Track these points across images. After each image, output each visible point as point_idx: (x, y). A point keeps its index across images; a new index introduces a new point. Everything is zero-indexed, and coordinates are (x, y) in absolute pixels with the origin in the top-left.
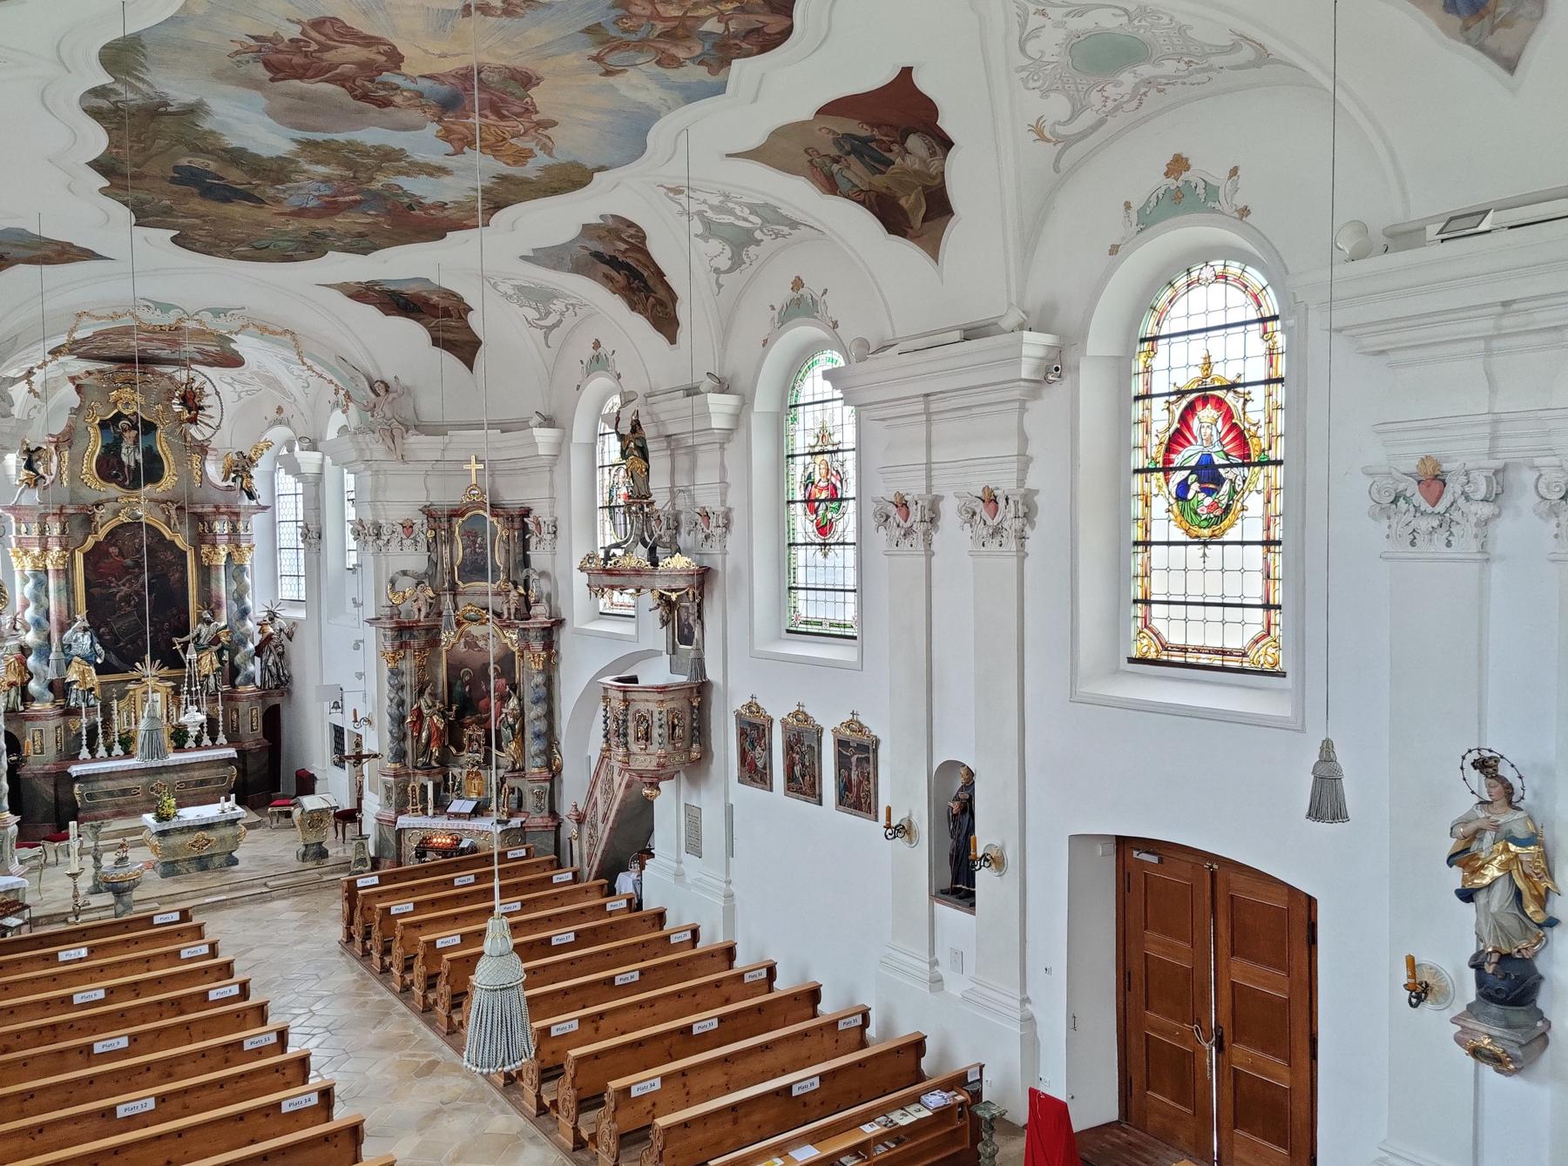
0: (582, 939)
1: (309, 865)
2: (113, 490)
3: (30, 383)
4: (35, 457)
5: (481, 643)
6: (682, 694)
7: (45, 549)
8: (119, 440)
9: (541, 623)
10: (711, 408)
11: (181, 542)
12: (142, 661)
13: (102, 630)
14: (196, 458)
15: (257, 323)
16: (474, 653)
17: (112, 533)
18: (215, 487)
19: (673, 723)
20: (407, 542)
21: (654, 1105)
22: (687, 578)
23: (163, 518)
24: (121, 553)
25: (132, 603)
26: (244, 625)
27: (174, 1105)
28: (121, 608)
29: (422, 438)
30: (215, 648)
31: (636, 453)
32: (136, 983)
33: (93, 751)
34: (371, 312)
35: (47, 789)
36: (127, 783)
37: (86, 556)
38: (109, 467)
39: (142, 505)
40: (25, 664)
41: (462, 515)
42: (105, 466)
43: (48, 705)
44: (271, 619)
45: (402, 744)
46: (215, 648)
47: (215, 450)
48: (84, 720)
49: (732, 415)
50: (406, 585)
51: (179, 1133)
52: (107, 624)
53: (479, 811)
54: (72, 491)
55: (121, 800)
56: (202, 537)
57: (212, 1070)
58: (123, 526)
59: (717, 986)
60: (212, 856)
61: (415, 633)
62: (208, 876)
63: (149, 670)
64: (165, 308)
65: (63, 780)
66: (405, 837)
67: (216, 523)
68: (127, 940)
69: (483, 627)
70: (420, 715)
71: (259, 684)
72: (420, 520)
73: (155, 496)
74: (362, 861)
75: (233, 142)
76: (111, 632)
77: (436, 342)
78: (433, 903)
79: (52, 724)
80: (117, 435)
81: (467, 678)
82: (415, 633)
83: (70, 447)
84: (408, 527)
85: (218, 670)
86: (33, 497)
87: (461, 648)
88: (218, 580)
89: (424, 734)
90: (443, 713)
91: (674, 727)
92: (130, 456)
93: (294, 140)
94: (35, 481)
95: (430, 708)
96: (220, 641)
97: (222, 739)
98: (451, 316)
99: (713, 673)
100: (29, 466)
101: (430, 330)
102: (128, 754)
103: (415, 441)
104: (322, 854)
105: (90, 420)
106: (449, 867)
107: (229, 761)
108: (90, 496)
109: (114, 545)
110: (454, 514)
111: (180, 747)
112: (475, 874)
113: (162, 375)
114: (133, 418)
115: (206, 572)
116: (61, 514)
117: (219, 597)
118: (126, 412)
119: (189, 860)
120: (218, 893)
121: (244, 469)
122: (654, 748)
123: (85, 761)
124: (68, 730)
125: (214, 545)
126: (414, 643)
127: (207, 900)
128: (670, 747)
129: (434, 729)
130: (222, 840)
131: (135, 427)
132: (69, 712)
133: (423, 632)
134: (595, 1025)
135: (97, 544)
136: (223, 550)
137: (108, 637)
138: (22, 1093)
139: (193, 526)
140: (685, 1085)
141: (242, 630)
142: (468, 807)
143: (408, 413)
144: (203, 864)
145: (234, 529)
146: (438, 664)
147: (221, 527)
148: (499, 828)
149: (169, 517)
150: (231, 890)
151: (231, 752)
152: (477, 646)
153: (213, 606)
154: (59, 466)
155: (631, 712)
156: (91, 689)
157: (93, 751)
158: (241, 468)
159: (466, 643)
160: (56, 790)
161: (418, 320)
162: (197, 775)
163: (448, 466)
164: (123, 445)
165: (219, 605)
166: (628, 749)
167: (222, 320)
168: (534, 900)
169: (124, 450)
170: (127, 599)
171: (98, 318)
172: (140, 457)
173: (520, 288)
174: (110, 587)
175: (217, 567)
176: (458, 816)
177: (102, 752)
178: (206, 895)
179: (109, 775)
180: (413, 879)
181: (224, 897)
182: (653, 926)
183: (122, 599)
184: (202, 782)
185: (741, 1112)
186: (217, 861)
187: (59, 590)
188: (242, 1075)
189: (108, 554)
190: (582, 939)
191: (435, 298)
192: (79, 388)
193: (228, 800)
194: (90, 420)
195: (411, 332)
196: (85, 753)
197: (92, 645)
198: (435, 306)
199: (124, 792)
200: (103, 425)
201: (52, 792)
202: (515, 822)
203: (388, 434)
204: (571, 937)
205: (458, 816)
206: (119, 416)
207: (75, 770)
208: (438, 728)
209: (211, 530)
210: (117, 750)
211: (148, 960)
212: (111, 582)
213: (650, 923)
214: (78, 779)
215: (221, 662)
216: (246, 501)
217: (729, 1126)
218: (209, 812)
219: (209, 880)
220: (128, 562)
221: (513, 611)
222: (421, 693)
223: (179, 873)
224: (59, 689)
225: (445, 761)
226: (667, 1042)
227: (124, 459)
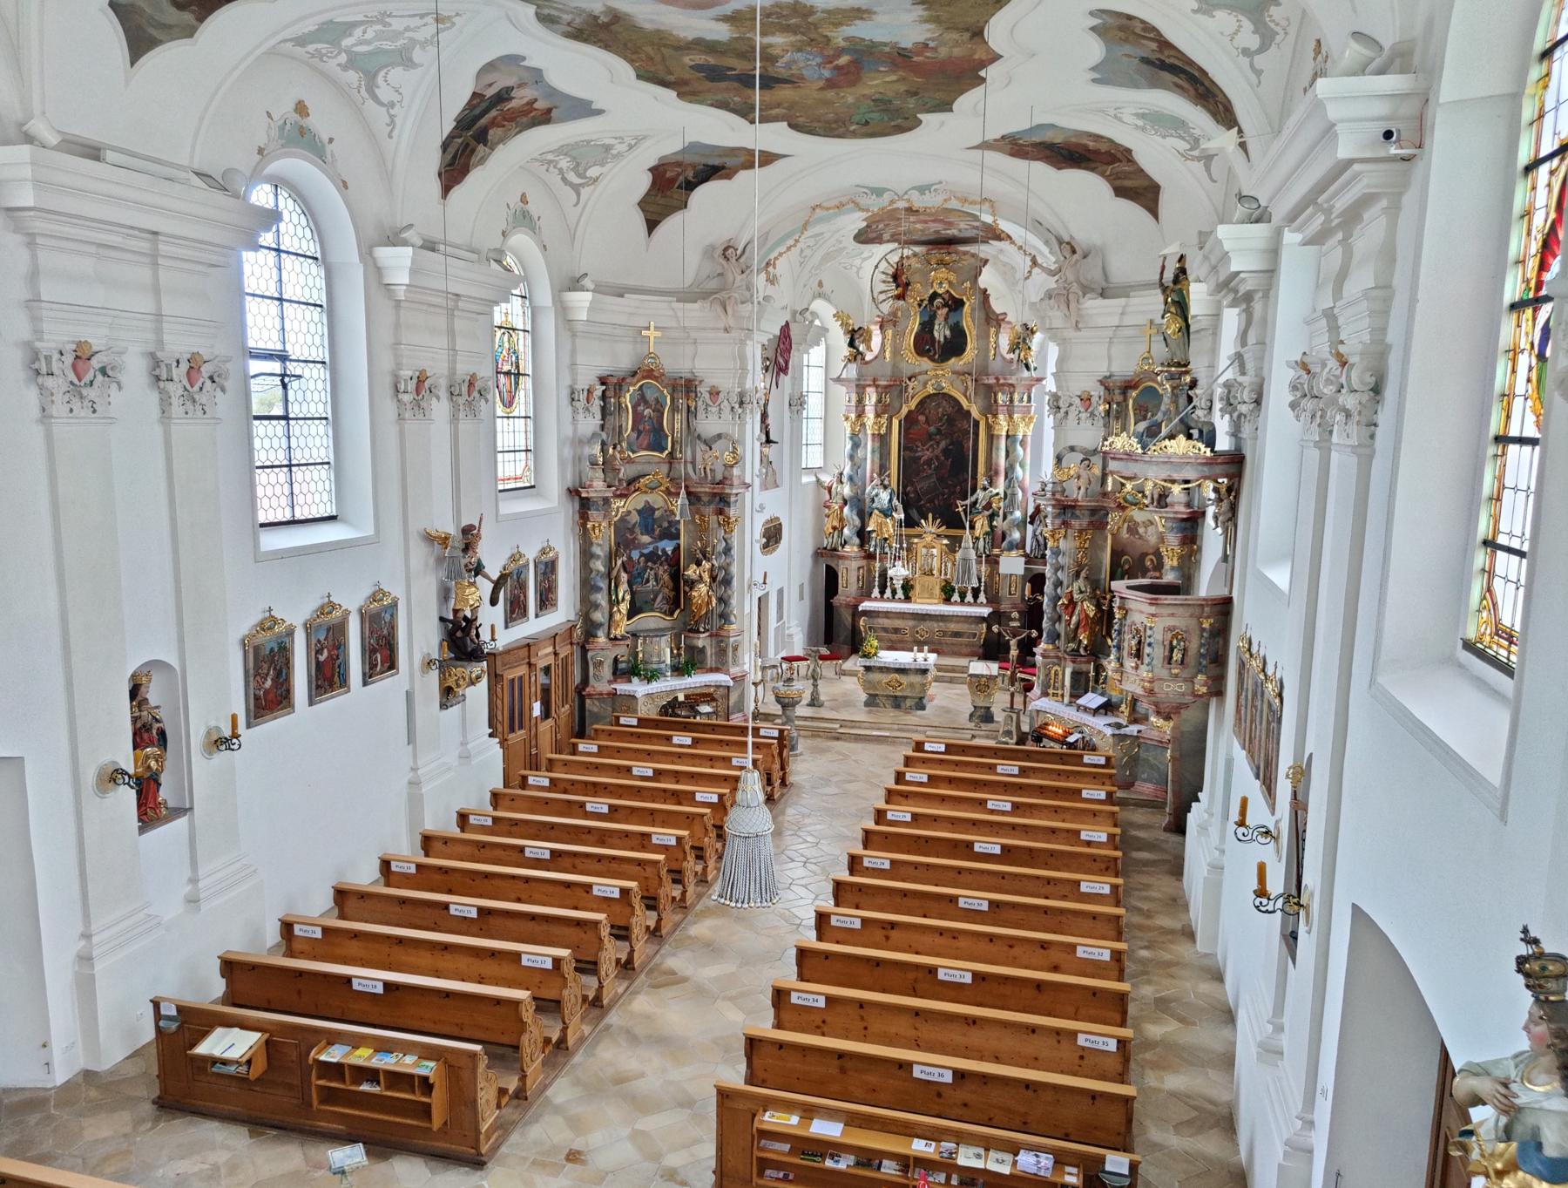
0: (1008, 854)
1: (972, 725)
2: (926, 364)
3: (1041, 266)
4: (856, 336)
5: (1141, 530)
6: (1191, 610)
7: (860, 414)
8: (933, 317)
9: (1176, 513)
10: (1226, 248)
11: (975, 413)
12: (926, 519)
14: (993, 330)
15: (959, 195)
16: (1135, 539)
17: (921, 403)
18: (1004, 358)
19: (1171, 642)
20: (1083, 416)
21: (824, 1022)
22: (1200, 468)
23: (962, 388)
24: (927, 422)
27: (567, 862)
29: (1100, 302)
30: (987, 513)
31: (1173, 309)
32: (677, 772)
33: (882, 592)
34: (1040, 169)
35: (847, 617)
36: (898, 623)
38: (924, 343)
39: (944, 378)
40: (842, 511)
41: (1135, 387)
43: (856, 549)
45: (1057, 625)
46: (987, 513)
47: (1009, 323)
48: (878, 565)
49: (1265, 251)
50: (1073, 462)
51: (527, 880)
53: (1108, 708)
54: (894, 365)
55: (894, 637)
56: (991, 409)
57: (632, 849)
58: (929, 396)
59: (1042, 947)
60: (905, 698)
61: (1078, 512)
62: (897, 713)
63: (929, 527)
64: (879, 192)
65: (856, 614)
66: (1041, 714)
67: (1000, 395)
68: (721, 741)
69: (1143, 513)
70: (1072, 603)
71: (1028, 551)
72: (1097, 392)
73: (957, 368)
74: (1008, 733)
75: (690, 36)
77: (1120, 192)
78: (951, 781)
79: (854, 565)
81: (1127, 567)
82: (1078, 512)
84: (1086, 400)
85: (987, 533)
86: (852, 371)
87: (1124, 534)
88: (998, 449)
89: (1074, 619)
90: (1098, 601)
91: (1172, 650)
92: (941, 332)
93: (718, 20)
94: (856, 356)
95: (1081, 592)
97: (982, 598)
98: (1120, 161)
99: (1235, 595)
100: (851, 344)
101: (1107, 178)
102: (908, 599)
103: (1093, 305)
104: (987, 717)
106: (1020, 755)
107: (983, 619)
108: (907, 370)
109: (922, 413)
110: (1127, 387)
111: (947, 600)
112: (1020, 767)
113: (965, 253)
114: (946, 297)
115: (991, 438)
116: (877, 387)
117: (997, 465)
118: (941, 291)
119: (887, 696)
120: (888, 729)
121: (1024, 340)
122: (1144, 672)
123: (876, 599)
124: (869, 571)
125: (995, 416)
126: (1076, 523)
127: (875, 733)
128: (1164, 673)
129: (1083, 616)
130: (911, 685)
131: (946, 305)
132: (870, 557)
133: (1087, 513)
134: (884, 932)
135: (910, 412)
136: (1002, 419)
138: (511, 819)
139: (988, 397)
140: (862, 1018)
142: (1101, 700)
143: (1096, 274)
144: (897, 702)
145: (1011, 400)
146: (1103, 548)
147: (1001, 398)
148: (1109, 731)
149: (967, 388)
150: (899, 730)
151: (986, 611)
152: (1138, 533)
154: (883, 344)
155: (1128, 622)
156: (886, 539)
157: (882, 592)
158: (1021, 343)
159: (1129, 530)
160: (853, 620)
161: (1092, 170)
162: (953, 627)
163: (1130, 332)
164: (937, 322)
165: (997, 473)
166: (1122, 665)
167: (927, 197)
168: (1031, 806)
169: (936, 327)
170: (929, 462)
171: (828, 209)
172: (948, 333)
173: (1142, 116)
175: (999, 437)
176: (1086, 709)
177: (888, 593)
178: (879, 729)
179: (887, 614)
180: (982, 757)
181: (887, 734)
182: (1107, 869)
184: (956, 634)
185: (849, 1064)
186: (909, 703)
187: (873, 451)
188: (614, 858)
189: (917, 421)
190: (1008, 854)
191: (1091, 145)
193: (921, 650)
195: (1087, 186)
196: (876, 593)
197: (890, 500)
198: (1097, 152)
199: (896, 631)
201: (850, 619)
202: (1133, 729)
203: (1062, 299)
204: (997, 850)
205: (1086, 709)
206: (934, 296)
207: (866, 605)
208: (1087, 616)
209: (996, 401)
210: (900, 594)
211: (711, 758)
213: (1103, 866)
214: (866, 613)
215: (991, 526)
216: (1026, 374)
217: (834, 1071)
218: (903, 658)
219: (888, 716)
220: (932, 429)
221: (1156, 497)
222: (1077, 575)
223: (877, 705)
224: (863, 535)
225: (1097, 651)
226: (911, 975)
227: (936, 334)
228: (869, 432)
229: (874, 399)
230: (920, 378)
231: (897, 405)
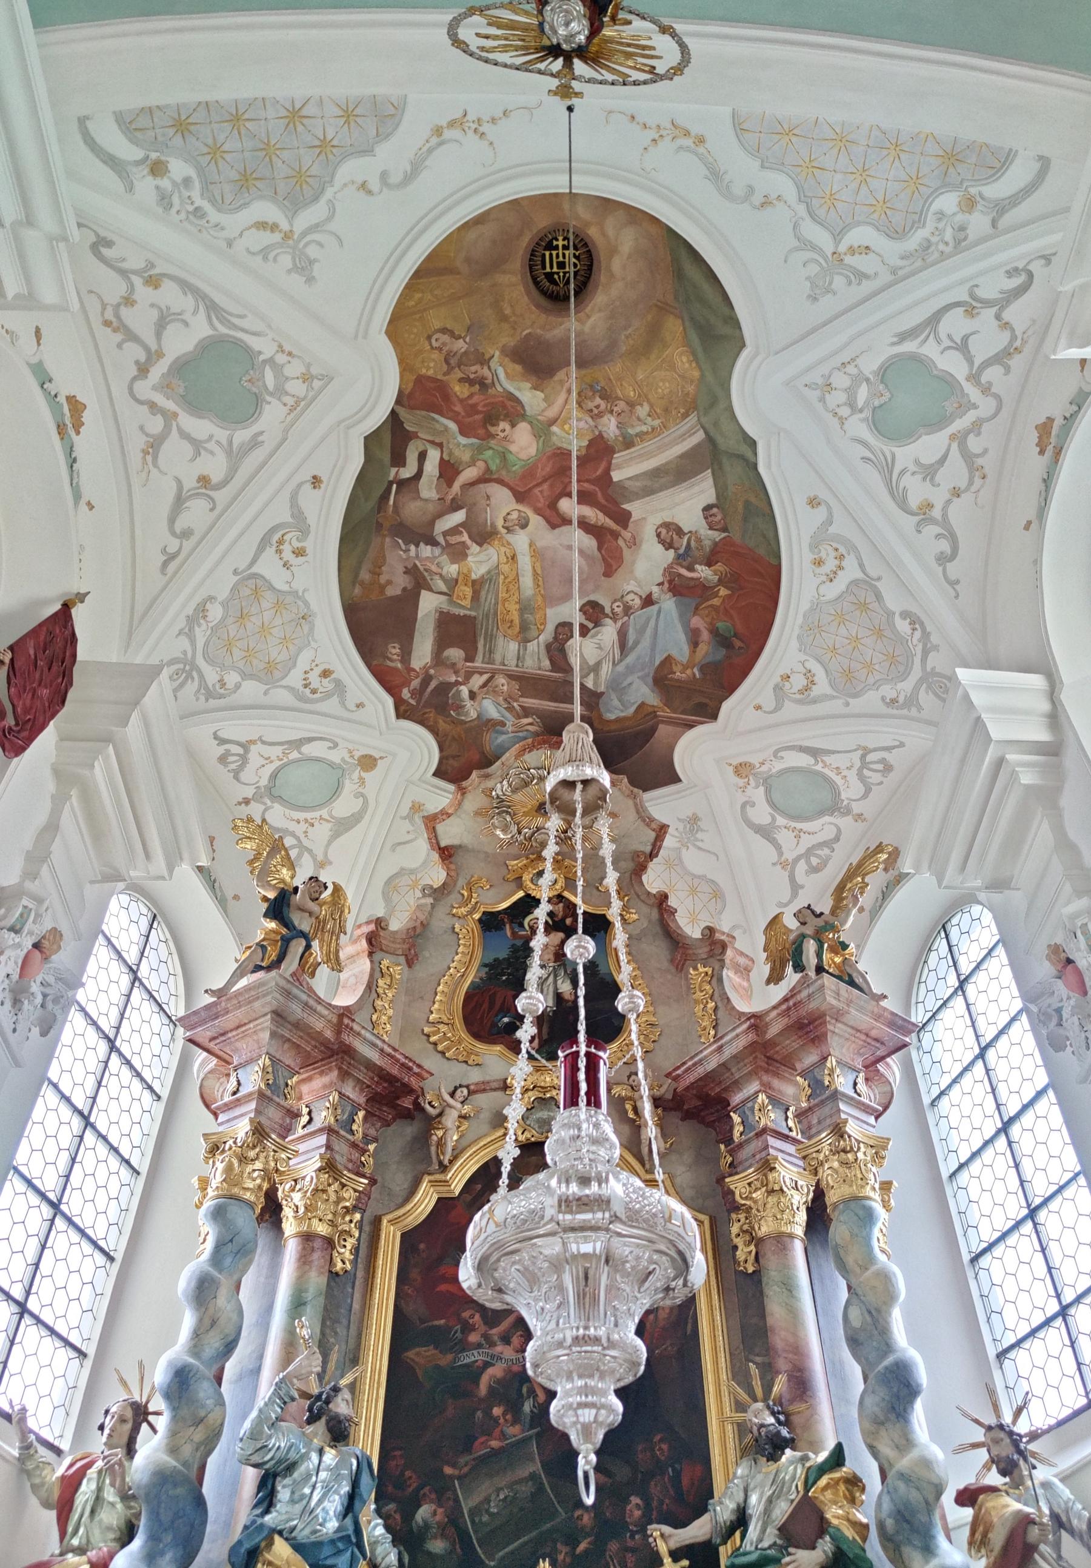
13: (424, 1512)
25: (527, 1407)
26: (906, 1443)
28: (490, 1426)
37: (409, 1240)
42: (486, 1006)
44: (1007, 1468)
52: (442, 1491)
76: (454, 1524)
80: (519, 943)
83: (410, 963)
88: (789, 1286)
96: (822, 1526)
105: (463, 910)
117: (798, 1351)
125: (767, 1166)
137: (437, 1546)
141: (904, 1463)
153: (780, 1385)
165: (801, 1385)
174: (464, 1346)
183: (496, 1394)
187: (297, 1305)
192: (447, 854)
194: (463, 910)
200: (490, 923)
212: (468, 1328)
228: (290, 1227)
229: (323, 1117)
230: (482, 1099)
231: (398, 1180)
